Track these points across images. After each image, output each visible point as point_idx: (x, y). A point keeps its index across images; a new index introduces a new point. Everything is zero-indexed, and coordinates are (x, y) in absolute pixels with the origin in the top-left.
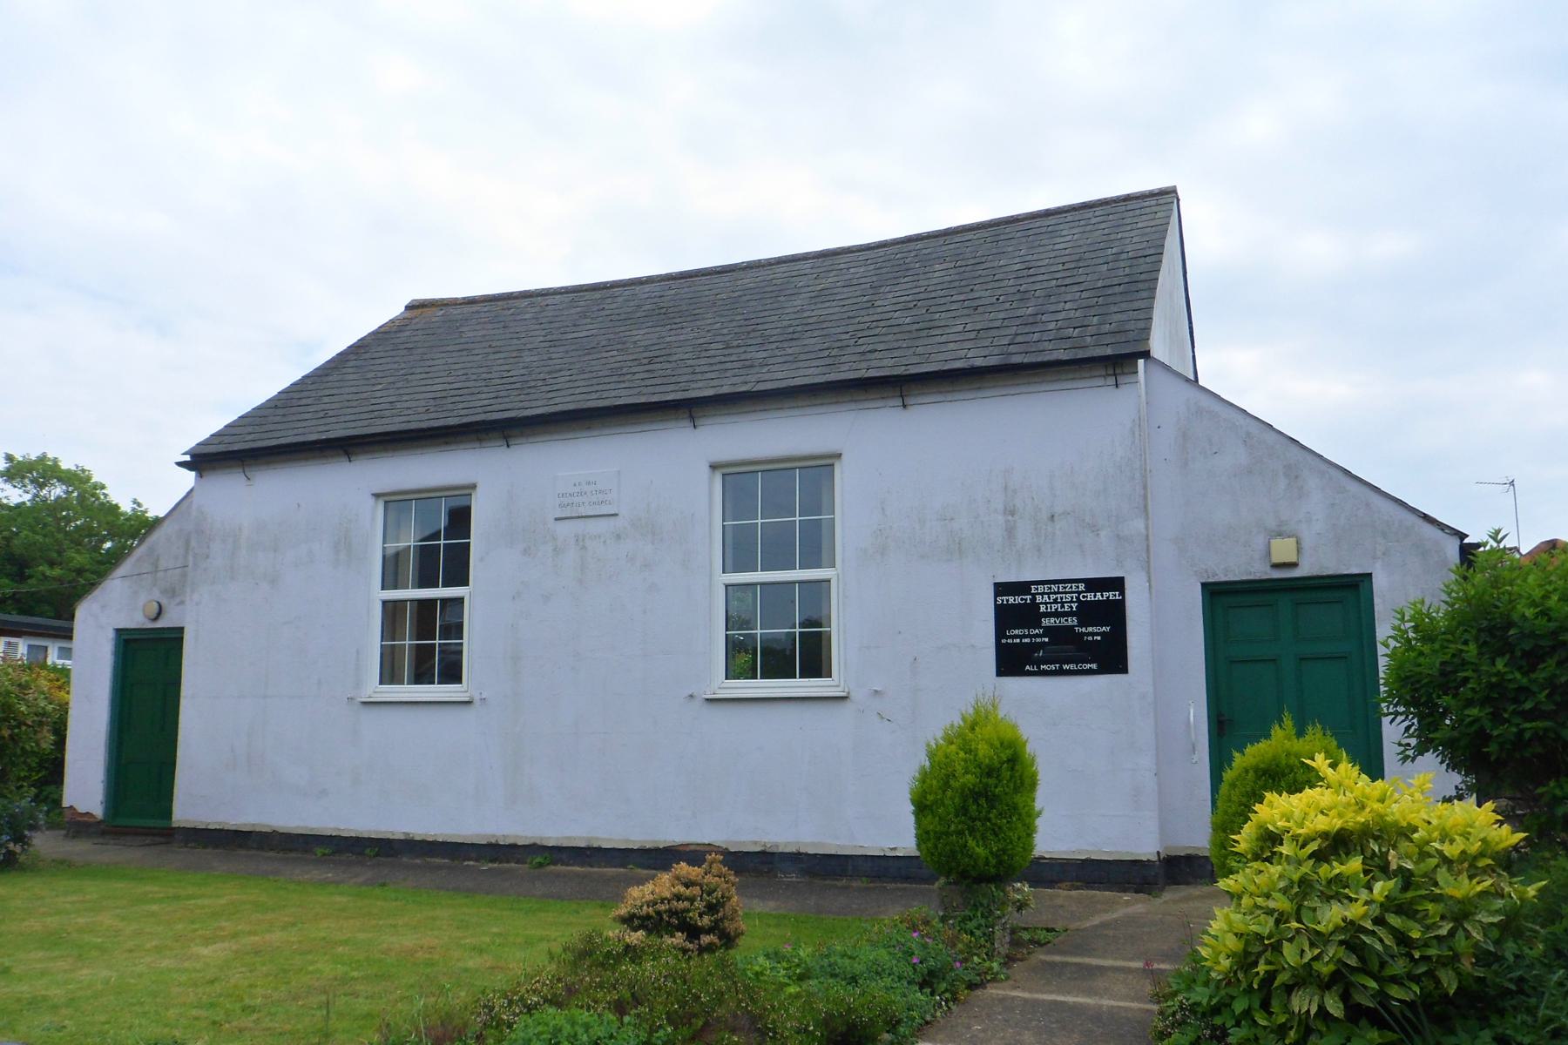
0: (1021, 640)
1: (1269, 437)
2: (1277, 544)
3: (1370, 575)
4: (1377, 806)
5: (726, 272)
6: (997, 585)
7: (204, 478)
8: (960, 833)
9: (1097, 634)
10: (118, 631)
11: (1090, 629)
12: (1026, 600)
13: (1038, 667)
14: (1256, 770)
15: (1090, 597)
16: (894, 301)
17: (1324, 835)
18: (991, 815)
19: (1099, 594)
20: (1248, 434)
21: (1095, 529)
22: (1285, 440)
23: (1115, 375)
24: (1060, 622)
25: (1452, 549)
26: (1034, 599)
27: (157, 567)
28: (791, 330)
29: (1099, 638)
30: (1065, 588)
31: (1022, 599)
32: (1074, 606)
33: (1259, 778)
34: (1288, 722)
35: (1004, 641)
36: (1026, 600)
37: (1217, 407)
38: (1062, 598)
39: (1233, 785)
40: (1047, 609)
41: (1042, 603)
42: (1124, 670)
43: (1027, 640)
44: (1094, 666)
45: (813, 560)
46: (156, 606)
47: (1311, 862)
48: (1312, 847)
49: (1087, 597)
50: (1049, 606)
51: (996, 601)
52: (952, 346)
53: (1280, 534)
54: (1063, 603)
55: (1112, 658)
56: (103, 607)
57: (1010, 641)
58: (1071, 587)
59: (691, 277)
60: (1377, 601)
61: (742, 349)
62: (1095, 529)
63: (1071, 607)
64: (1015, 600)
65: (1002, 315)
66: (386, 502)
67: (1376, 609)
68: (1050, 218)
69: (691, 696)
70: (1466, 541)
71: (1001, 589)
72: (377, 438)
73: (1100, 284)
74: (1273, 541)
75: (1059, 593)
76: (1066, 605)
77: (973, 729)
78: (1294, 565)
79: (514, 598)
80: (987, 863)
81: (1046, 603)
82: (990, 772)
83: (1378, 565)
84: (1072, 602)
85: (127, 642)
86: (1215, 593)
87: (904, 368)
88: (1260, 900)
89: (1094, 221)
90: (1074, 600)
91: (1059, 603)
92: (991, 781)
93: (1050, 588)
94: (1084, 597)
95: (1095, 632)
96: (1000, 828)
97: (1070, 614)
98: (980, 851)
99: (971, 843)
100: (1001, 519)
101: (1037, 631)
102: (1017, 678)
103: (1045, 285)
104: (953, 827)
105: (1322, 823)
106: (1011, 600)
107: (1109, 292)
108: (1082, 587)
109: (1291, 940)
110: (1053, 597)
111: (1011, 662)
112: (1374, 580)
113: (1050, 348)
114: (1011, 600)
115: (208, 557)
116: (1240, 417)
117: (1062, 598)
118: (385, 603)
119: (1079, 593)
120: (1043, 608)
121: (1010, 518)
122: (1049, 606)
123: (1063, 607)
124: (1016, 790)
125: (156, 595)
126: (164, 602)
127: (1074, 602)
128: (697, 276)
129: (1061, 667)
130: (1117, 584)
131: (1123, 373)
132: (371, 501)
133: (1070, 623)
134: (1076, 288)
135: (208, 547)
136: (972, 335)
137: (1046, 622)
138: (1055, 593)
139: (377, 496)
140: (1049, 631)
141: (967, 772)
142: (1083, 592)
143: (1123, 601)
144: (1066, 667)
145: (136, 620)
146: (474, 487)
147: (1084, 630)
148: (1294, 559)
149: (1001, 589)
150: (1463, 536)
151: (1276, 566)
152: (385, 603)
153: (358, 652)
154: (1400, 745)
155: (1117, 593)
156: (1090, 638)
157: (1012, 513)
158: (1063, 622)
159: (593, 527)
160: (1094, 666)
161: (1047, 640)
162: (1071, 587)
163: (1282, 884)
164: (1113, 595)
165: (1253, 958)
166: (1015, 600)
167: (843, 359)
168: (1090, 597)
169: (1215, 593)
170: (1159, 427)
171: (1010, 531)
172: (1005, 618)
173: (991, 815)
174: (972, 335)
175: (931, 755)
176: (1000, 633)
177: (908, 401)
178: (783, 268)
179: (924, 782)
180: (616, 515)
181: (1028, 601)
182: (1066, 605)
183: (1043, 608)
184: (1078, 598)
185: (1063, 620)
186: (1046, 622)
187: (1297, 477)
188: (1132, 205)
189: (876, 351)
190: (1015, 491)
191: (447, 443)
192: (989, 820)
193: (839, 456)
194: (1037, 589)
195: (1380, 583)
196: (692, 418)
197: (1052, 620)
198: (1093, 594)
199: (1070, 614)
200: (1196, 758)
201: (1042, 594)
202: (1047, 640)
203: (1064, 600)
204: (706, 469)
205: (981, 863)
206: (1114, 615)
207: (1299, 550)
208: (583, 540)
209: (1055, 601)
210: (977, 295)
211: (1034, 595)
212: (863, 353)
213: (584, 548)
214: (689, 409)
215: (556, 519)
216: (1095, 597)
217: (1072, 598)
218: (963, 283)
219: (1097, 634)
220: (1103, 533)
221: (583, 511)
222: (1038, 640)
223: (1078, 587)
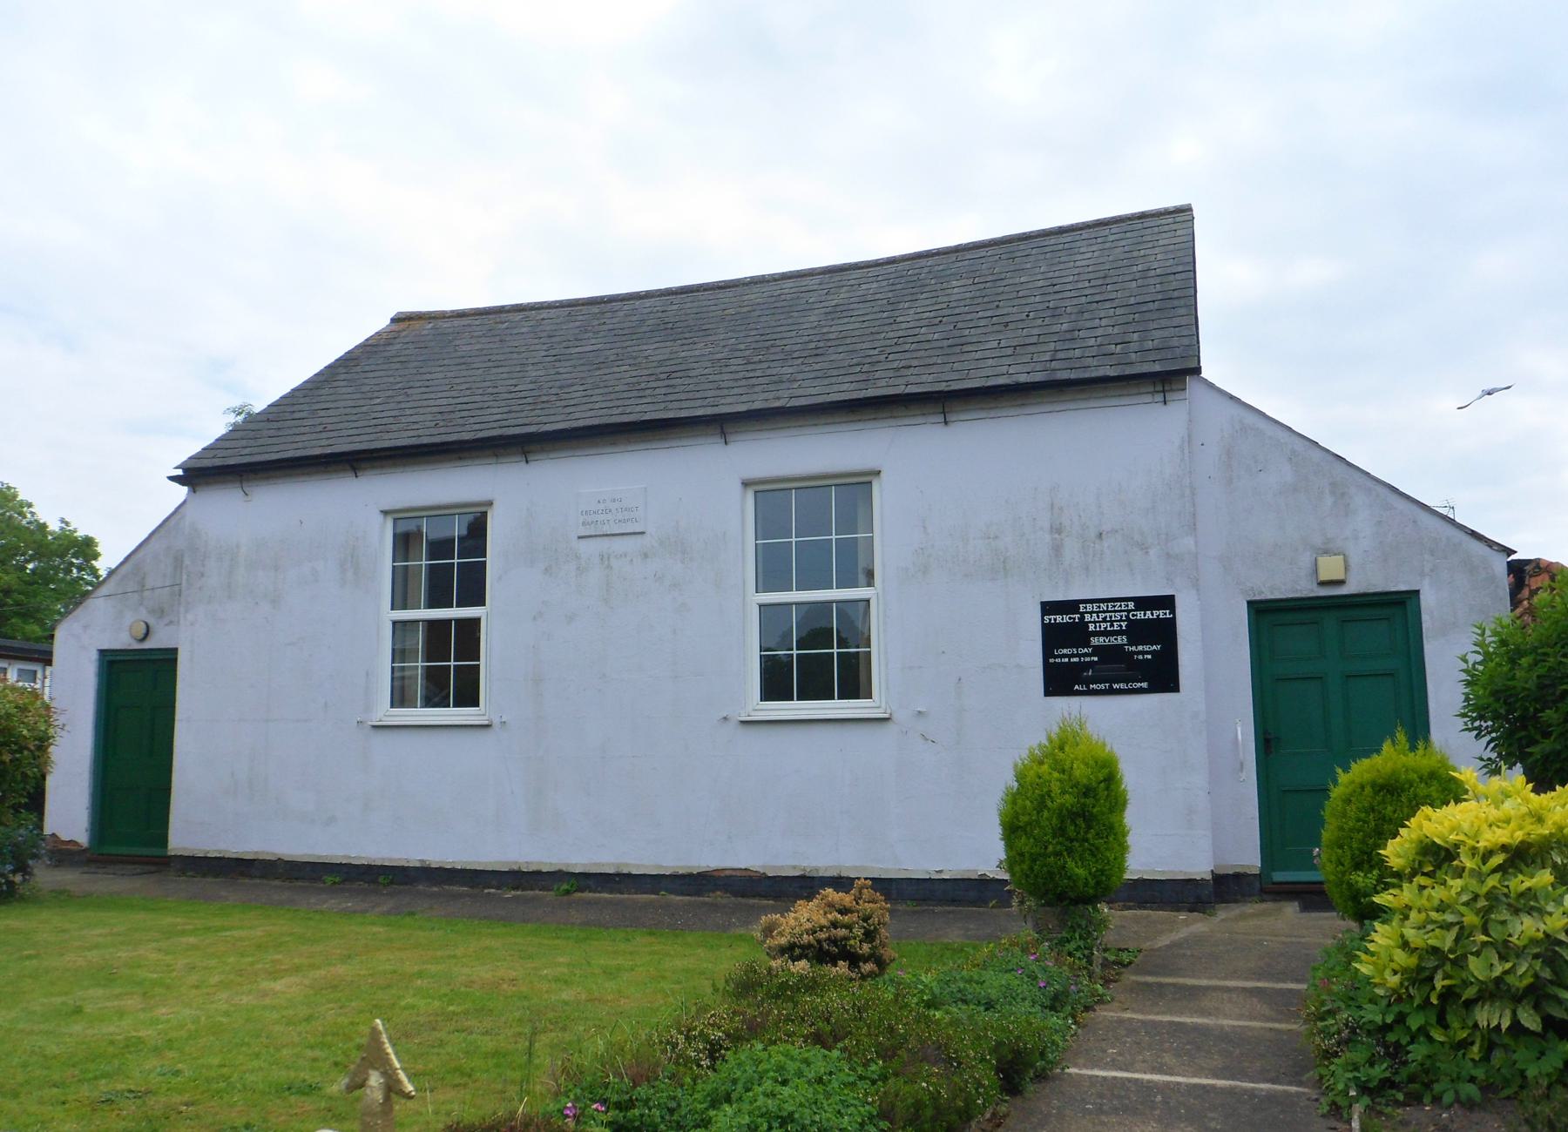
0: (1069, 660)
1: (1316, 455)
2: (1323, 561)
3: (1417, 592)
5: (729, 287)
7: (198, 493)
8: (1058, 854)
9: (1147, 653)
10: (102, 652)
12: (1074, 619)
13: (1088, 687)
14: (1373, 784)
15: (1140, 615)
16: (917, 317)
17: (1504, 848)
18: (1090, 836)
19: (1149, 612)
20: (1293, 451)
21: (1145, 549)
22: (1331, 458)
23: (1164, 391)
24: (1109, 641)
25: (1500, 565)
26: (1082, 618)
27: (143, 586)
28: (813, 345)
29: (1149, 657)
30: (1114, 606)
31: (1070, 618)
33: (1376, 793)
34: (1401, 737)
35: (1052, 660)
36: (1074, 619)
37: (1262, 424)
38: (1111, 617)
39: (1348, 801)
40: (1095, 628)
41: (1091, 622)
43: (1075, 660)
44: (1145, 685)
45: (847, 582)
46: (144, 626)
47: (1498, 876)
48: (1498, 859)
49: (1136, 615)
50: (1098, 624)
51: (1043, 620)
52: (990, 362)
53: (1326, 552)
54: (1112, 622)
55: (1163, 676)
56: (86, 627)
57: (1058, 660)
58: (1121, 606)
59: (692, 292)
60: (1425, 617)
61: (765, 365)
62: (1145, 549)
63: (1121, 626)
64: (1063, 619)
65: (1036, 331)
66: (395, 520)
67: (1424, 626)
68: (1064, 235)
69: (725, 718)
70: (1513, 557)
71: (1048, 608)
73: (1132, 300)
74: (1320, 559)
75: (1108, 611)
76: (1115, 624)
77: (1062, 748)
78: (1341, 583)
79: (535, 618)
80: (1086, 885)
81: (1095, 622)
82: (1088, 791)
83: (1427, 581)
84: (1121, 620)
85: (111, 663)
86: (1263, 613)
87: (944, 384)
88: (1434, 915)
89: (1111, 238)
90: (1124, 618)
91: (1108, 621)
92: (1089, 801)
93: (1099, 607)
94: (1133, 615)
95: (1146, 651)
96: (1097, 849)
97: (1120, 633)
98: (1081, 872)
99: (1070, 864)
100: (1047, 537)
101: (1086, 650)
102: (1066, 697)
103: (1075, 301)
104: (1050, 848)
105: (1502, 836)
106: (1059, 619)
107: (1144, 309)
108: (1131, 605)
109: (1477, 954)
110: (1102, 616)
111: (1059, 681)
112: (1422, 597)
113: (1095, 364)
114: (1059, 619)
115: (202, 575)
116: (1287, 434)
117: (1111, 617)
118: (395, 623)
119: (1129, 611)
120: (1091, 627)
121: (1057, 536)
122: (1098, 624)
123: (1112, 625)
124: (1111, 811)
125: (144, 614)
126: (152, 622)
127: (1124, 621)
128: (698, 291)
129: (1111, 687)
130: (1167, 602)
131: (1172, 390)
132: (380, 517)
133: (1120, 642)
134: (1108, 305)
135: (204, 566)
136: (1010, 351)
137: (1095, 641)
138: (1104, 612)
139: (385, 513)
140: (1098, 650)
141: (1064, 792)
142: (1132, 610)
143: (1174, 619)
144: (1115, 686)
145: (122, 640)
146: (490, 504)
147: (1134, 648)
148: (1341, 577)
149: (1048, 608)
150: (1510, 552)
151: (1323, 584)
152: (395, 623)
153: (367, 674)
154: (1482, 759)
155: (1168, 611)
156: (1140, 657)
157: (1059, 531)
158: (1113, 641)
159: (619, 545)
160: (1145, 685)
161: (1096, 659)
162: (1121, 606)
163: (1465, 898)
164: (1162, 614)
165: (1427, 974)
166: (1063, 619)
167: (877, 375)
168: (1140, 615)
169: (1263, 613)
170: (1202, 445)
171: (1057, 549)
172: (1053, 637)
173: (1090, 836)
174: (1010, 351)
175: (1020, 777)
176: (1048, 651)
177: (950, 417)
178: (789, 284)
179: (1014, 803)
180: (643, 533)
181: (1077, 620)
182: (1115, 624)
183: (1091, 627)
184: (1127, 617)
185: (1112, 639)
186: (1095, 641)
187: (1343, 494)
188: (1149, 223)
189: (911, 367)
190: (1061, 509)
191: (460, 458)
192: (1087, 840)
193: (879, 473)
194: (1086, 608)
195: (1428, 601)
196: (724, 434)
197: (1101, 639)
198: (1142, 612)
199: (1120, 633)
200: (1243, 776)
201: (1091, 613)
202: (1096, 659)
203: (1113, 619)
204: (738, 486)
205: (1080, 884)
206: (1166, 633)
207: (1346, 569)
208: (609, 558)
209: (1104, 620)
210: (1005, 311)
211: (1082, 614)
212: (897, 369)
213: (609, 567)
214: (722, 425)
215: (579, 538)
216: (1145, 615)
217: (1122, 617)
218: (986, 300)
219: (1147, 653)
220: (1152, 552)
221: (607, 529)
222: (1087, 659)
223: (1127, 606)
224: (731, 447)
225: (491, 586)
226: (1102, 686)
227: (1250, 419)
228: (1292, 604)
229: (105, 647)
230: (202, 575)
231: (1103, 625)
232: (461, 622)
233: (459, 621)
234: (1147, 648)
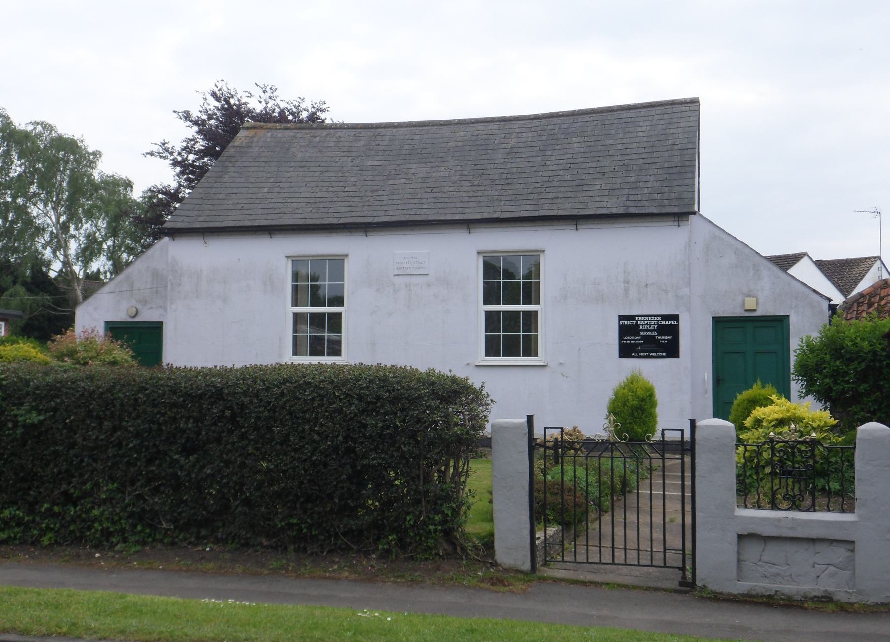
1: (747, 251)
2: (747, 300)
3: (788, 316)
4: (793, 411)
5: (447, 125)
6: (619, 316)
8: (630, 423)
9: (666, 340)
11: (663, 337)
13: (638, 354)
14: (748, 400)
15: (663, 323)
16: (557, 162)
17: (777, 420)
18: (643, 417)
19: (667, 322)
20: (737, 249)
21: (666, 292)
22: (753, 253)
23: (679, 221)
25: (825, 305)
26: (637, 323)
27: (133, 287)
28: (504, 176)
29: (667, 342)
32: (656, 326)
33: (749, 403)
34: (759, 382)
35: (622, 342)
37: (724, 236)
39: (739, 406)
42: (678, 356)
43: (633, 342)
44: (664, 354)
45: (527, 301)
46: (135, 310)
47: (773, 428)
48: (773, 423)
51: (619, 323)
52: (597, 198)
53: (749, 296)
54: (650, 325)
55: (672, 350)
57: (625, 342)
59: (425, 126)
60: (791, 327)
61: (482, 188)
62: (666, 292)
65: (619, 180)
66: (292, 260)
67: (790, 331)
68: (632, 111)
69: (468, 364)
70: (831, 303)
71: (622, 318)
72: (288, 227)
73: (666, 165)
74: (746, 299)
77: (632, 383)
78: (754, 310)
79: (371, 314)
80: (641, 435)
81: (642, 325)
82: (643, 400)
83: (793, 311)
84: (654, 325)
86: (719, 323)
87: (576, 211)
88: (755, 440)
89: (656, 117)
92: (643, 404)
95: (665, 339)
96: (646, 422)
98: (639, 430)
99: (635, 427)
100: (622, 285)
103: (637, 162)
104: (628, 421)
105: (776, 416)
106: (626, 323)
107: (672, 172)
108: (659, 318)
109: (765, 451)
110: (646, 322)
111: (626, 351)
112: (790, 318)
113: (648, 205)
114: (626, 323)
115: (180, 285)
116: (733, 242)
119: (658, 321)
120: (641, 327)
121: (626, 285)
123: (650, 327)
124: (651, 408)
125: (134, 303)
126: (139, 307)
128: (429, 126)
129: (649, 354)
130: (676, 317)
131: (682, 220)
132: (285, 259)
134: (654, 167)
135: (181, 280)
136: (606, 192)
137: (642, 334)
138: (647, 320)
139: (288, 257)
140: (643, 338)
141: (633, 400)
143: (678, 325)
144: (651, 354)
146: (347, 256)
147: (660, 338)
148: (755, 308)
149: (622, 318)
150: (830, 300)
151: (746, 310)
153: (280, 339)
154: (799, 392)
156: (663, 342)
157: (628, 283)
158: (650, 334)
159: (415, 279)
160: (664, 354)
163: (763, 434)
165: (752, 458)
167: (543, 201)
168: (663, 323)
169: (719, 323)
171: (627, 291)
172: (623, 331)
173: (643, 417)
174: (606, 192)
175: (616, 394)
176: (621, 338)
177: (579, 227)
178: (481, 127)
179: (613, 403)
180: (427, 274)
183: (641, 327)
184: (657, 323)
185: (650, 333)
186: (642, 334)
187: (758, 270)
188: (677, 108)
189: (558, 198)
190: (629, 273)
191: (330, 232)
192: (642, 418)
193: (544, 251)
195: (793, 320)
196: (468, 228)
197: (645, 333)
200: (707, 396)
201: (641, 321)
204: (475, 253)
205: (639, 435)
206: (674, 331)
207: (757, 304)
208: (410, 286)
209: (647, 324)
210: (602, 164)
211: (637, 321)
212: (552, 199)
213: (410, 290)
214: (468, 224)
215: (395, 275)
218: (592, 154)
219: (666, 340)
220: (670, 294)
221: (409, 272)
222: (639, 342)
224: (472, 234)
225: (348, 297)
226: (645, 354)
227: (718, 232)
228: (733, 318)
230: (180, 285)
231: (646, 327)
232: (331, 315)
233: (330, 314)
234: (666, 338)
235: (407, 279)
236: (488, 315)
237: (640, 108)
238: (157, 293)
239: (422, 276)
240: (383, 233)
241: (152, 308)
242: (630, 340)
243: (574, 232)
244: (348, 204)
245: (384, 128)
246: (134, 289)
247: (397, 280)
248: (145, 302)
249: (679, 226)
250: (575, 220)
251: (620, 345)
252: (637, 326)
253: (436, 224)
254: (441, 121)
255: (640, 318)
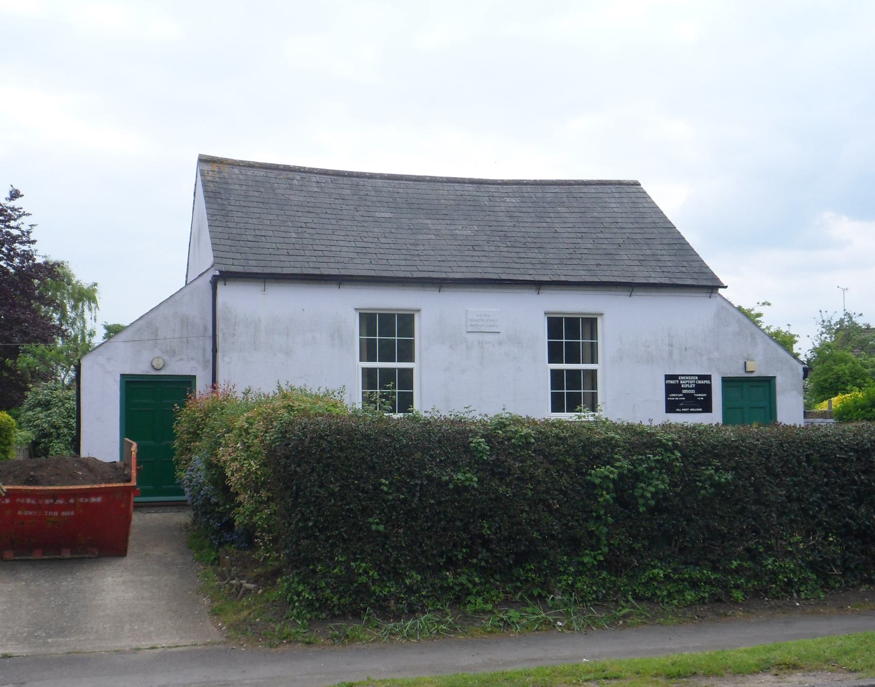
6: (666, 376)
7: (227, 285)
10: (123, 376)
11: (699, 395)
21: (701, 355)
26: (679, 382)
27: (157, 335)
32: (694, 385)
42: (711, 412)
43: (677, 399)
44: (701, 410)
56: (109, 359)
71: (668, 377)
78: (752, 372)
79: (445, 370)
83: (779, 373)
85: (127, 382)
95: (701, 396)
97: (692, 389)
108: (697, 378)
118: (363, 369)
120: (683, 386)
125: (158, 353)
126: (166, 358)
135: (235, 330)
137: (684, 391)
139: (356, 309)
140: (685, 395)
144: (691, 410)
145: (141, 368)
147: (697, 395)
152: (363, 369)
157: (672, 346)
160: (701, 410)
164: (707, 382)
168: (700, 382)
171: (671, 354)
176: (667, 396)
180: (499, 332)
183: (683, 386)
191: (403, 286)
195: (779, 381)
199: (692, 389)
204: (543, 314)
209: (687, 383)
213: (482, 347)
214: (538, 285)
215: (468, 332)
219: (702, 397)
222: (681, 399)
224: (540, 295)
225: (420, 354)
226: (686, 410)
227: (725, 304)
228: (737, 379)
229: (128, 372)
230: (234, 335)
231: (687, 385)
232: (402, 371)
234: (702, 395)
235: (477, 336)
236: (554, 373)
237: (453, 182)
238: (187, 343)
239: (494, 334)
240: (455, 290)
241: (182, 359)
242: (675, 397)
243: (628, 298)
244: (403, 257)
245: (415, 180)
246: (158, 338)
247: (470, 337)
248: (173, 353)
249: (630, 296)
250: (631, 287)
251: (667, 401)
252: (680, 384)
253: (520, 284)
254: (414, 176)
255: (683, 378)
